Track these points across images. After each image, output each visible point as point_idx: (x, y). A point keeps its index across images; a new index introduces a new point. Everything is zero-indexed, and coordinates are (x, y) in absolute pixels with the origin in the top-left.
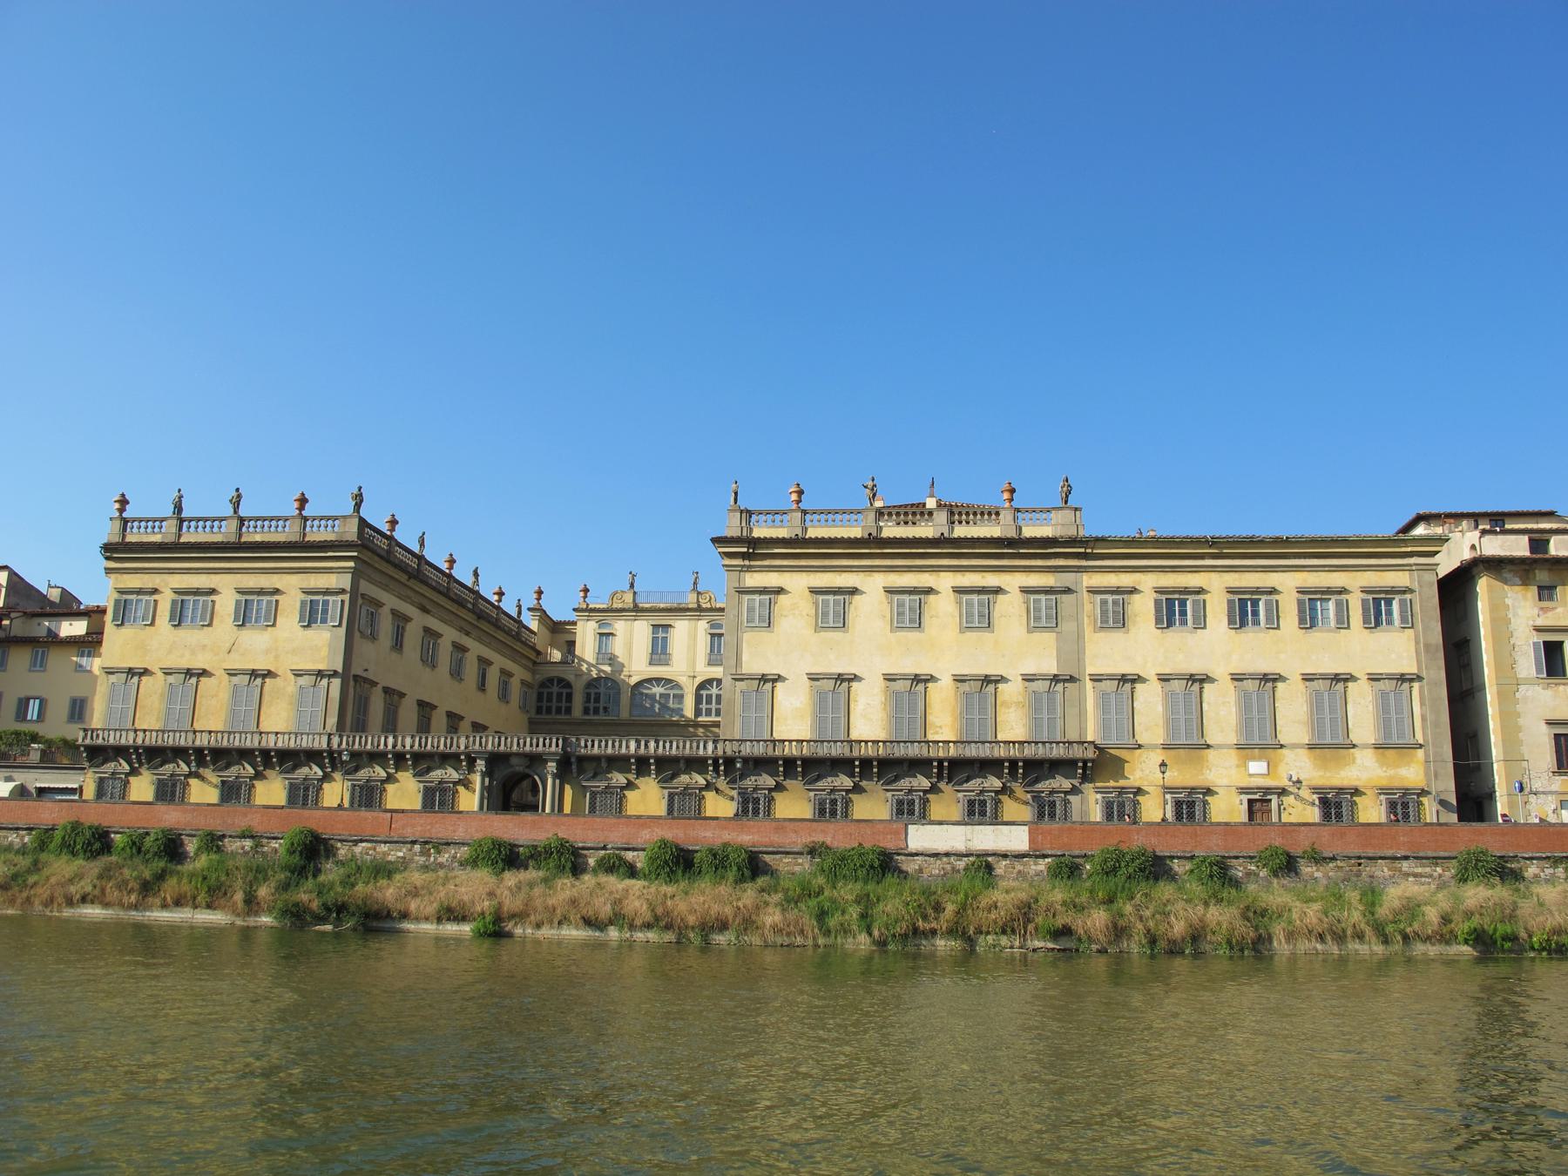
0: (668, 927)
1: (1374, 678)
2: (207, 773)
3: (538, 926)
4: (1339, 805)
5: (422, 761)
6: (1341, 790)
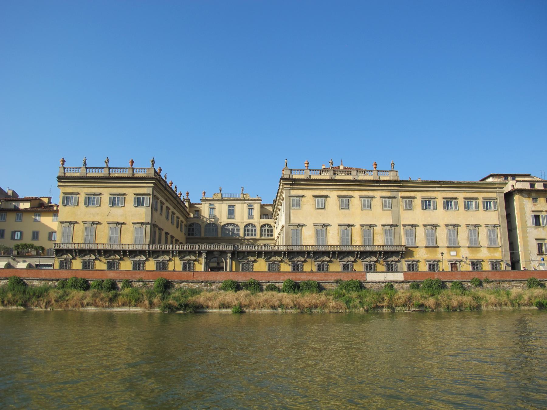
0: (299, 308)
1: (487, 226)
2: (102, 258)
3: (254, 309)
4: (477, 265)
5: (182, 254)
6: (478, 260)
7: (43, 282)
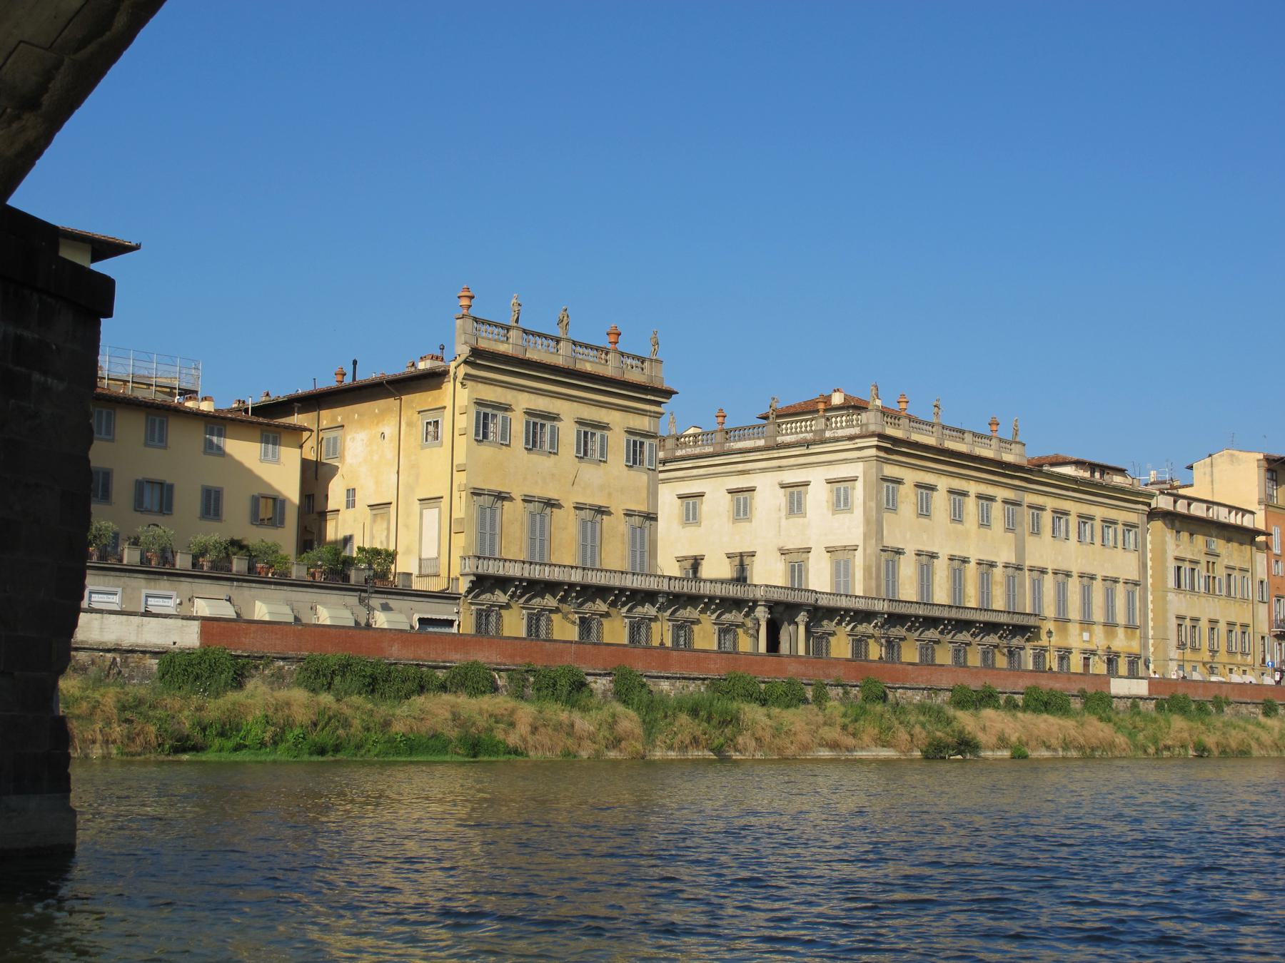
7: (678, 683)
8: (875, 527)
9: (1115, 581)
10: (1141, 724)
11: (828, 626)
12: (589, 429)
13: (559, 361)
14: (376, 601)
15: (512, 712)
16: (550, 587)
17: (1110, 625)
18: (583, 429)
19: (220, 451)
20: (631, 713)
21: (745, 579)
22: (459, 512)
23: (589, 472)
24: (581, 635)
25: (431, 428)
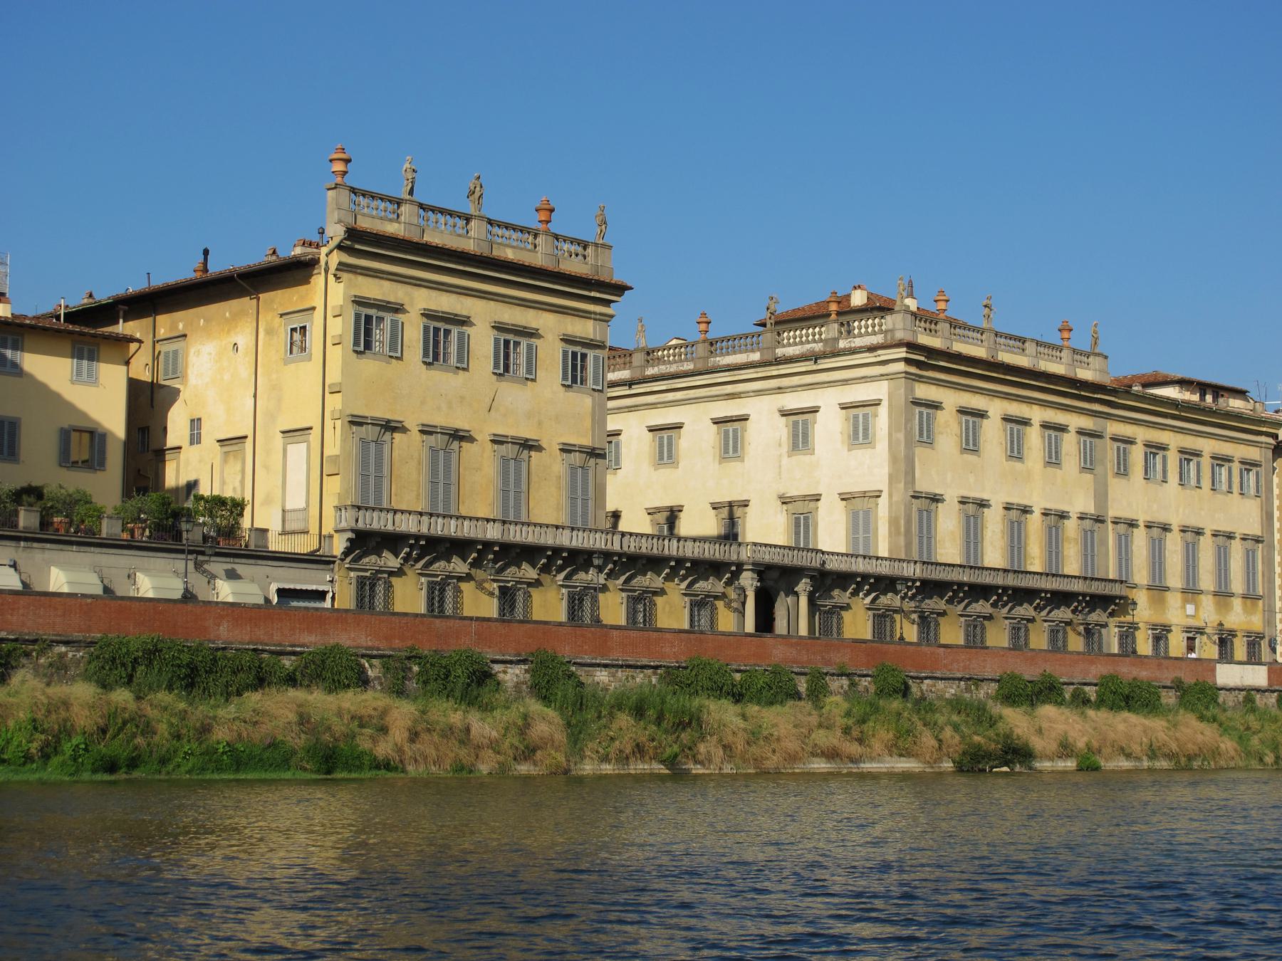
8: (904, 467)
9: (1230, 536)
10: (1255, 725)
11: (839, 596)
12: (511, 339)
13: (470, 246)
14: (218, 566)
15: (384, 713)
16: (459, 547)
17: (1223, 595)
18: (503, 336)
19: (17, 370)
20: (551, 713)
21: (735, 537)
22: (333, 449)
23: (513, 395)
24: (502, 610)
25: (297, 336)
